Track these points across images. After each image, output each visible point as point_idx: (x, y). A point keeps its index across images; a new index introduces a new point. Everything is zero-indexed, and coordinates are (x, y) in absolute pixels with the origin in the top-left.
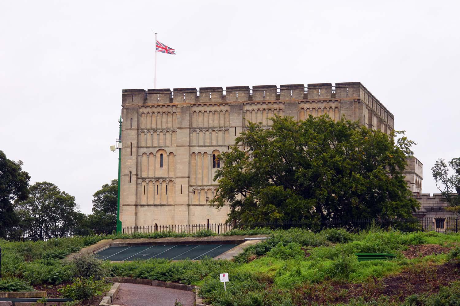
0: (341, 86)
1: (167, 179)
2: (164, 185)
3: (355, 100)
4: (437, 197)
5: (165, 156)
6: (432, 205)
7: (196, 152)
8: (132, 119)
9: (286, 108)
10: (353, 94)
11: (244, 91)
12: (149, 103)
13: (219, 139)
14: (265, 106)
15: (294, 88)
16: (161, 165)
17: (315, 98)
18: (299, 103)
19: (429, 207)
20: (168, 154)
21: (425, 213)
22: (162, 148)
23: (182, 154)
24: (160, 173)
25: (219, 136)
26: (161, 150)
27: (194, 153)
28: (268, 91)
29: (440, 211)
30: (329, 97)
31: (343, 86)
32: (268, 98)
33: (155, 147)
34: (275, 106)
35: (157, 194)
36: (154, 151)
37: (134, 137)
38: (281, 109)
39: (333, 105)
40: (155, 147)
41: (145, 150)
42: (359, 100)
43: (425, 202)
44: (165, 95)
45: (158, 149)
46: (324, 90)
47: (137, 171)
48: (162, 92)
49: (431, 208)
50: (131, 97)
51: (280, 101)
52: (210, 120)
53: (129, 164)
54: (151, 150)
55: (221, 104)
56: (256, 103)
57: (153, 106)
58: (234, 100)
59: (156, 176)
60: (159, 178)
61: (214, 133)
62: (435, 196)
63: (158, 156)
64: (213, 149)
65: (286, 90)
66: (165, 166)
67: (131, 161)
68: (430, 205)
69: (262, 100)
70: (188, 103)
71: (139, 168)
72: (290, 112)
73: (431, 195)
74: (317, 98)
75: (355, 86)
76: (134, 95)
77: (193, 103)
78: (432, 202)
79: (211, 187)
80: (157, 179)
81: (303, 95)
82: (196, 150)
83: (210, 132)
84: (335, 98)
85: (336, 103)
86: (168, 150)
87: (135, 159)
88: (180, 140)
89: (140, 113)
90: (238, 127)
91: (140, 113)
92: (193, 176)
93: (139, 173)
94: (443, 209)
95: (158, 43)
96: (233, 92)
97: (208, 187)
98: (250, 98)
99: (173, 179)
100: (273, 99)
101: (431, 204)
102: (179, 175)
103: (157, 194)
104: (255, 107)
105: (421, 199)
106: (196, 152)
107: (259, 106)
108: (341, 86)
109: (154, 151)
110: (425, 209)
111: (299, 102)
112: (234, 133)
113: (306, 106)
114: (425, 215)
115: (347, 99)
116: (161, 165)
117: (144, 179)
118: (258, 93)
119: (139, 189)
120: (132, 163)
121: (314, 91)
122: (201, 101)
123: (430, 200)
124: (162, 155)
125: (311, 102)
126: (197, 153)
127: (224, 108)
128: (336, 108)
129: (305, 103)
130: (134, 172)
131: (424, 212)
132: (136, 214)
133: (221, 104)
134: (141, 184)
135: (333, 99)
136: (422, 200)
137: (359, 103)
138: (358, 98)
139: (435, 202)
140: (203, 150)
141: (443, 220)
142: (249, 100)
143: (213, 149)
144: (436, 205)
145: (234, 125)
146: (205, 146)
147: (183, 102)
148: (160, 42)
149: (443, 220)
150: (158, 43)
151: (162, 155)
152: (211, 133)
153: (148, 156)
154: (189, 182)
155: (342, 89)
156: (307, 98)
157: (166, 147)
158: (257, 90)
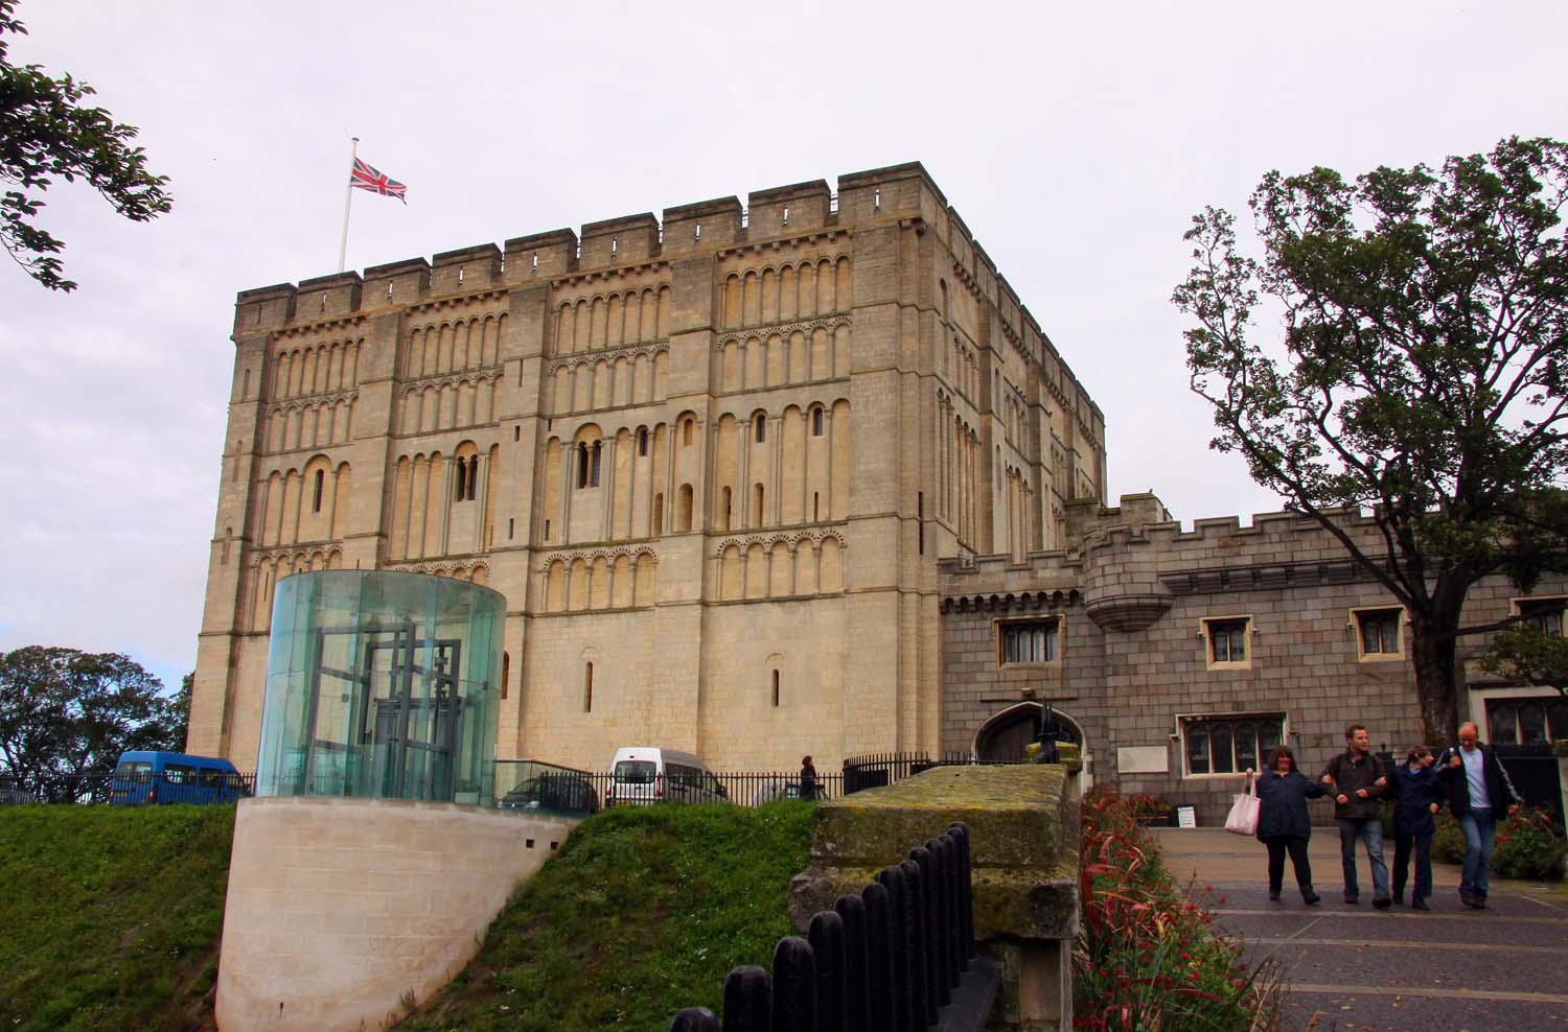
0: (854, 183)
1: (327, 547)
3: (904, 224)
4: (1209, 533)
6: (1192, 566)
7: (411, 453)
8: (248, 371)
9: (676, 276)
10: (898, 203)
11: (558, 243)
12: (300, 322)
13: (479, 404)
14: (616, 285)
15: (706, 211)
16: (317, 508)
17: (771, 234)
18: (722, 260)
19: (1180, 573)
20: (335, 468)
21: (1163, 601)
22: (323, 452)
23: (368, 461)
25: (480, 397)
27: (404, 457)
28: (627, 233)
29: (1226, 587)
30: (817, 226)
31: (864, 182)
32: (625, 255)
33: (305, 450)
34: (649, 279)
37: (249, 424)
38: (664, 287)
39: (831, 250)
40: (305, 450)
42: (917, 221)
43: (1162, 557)
44: (342, 292)
45: (310, 455)
46: (800, 203)
47: (248, 524)
48: (334, 284)
49: (1187, 577)
50: (254, 310)
51: (660, 259)
52: (457, 351)
55: (488, 295)
56: (588, 278)
57: (308, 328)
58: (527, 277)
59: (301, 540)
60: (305, 546)
61: (464, 389)
62: (1203, 527)
63: (312, 476)
64: (456, 438)
65: (681, 223)
66: (326, 507)
67: (233, 496)
68: (1186, 566)
69: (607, 264)
70: (399, 306)
71: (258, 519)
72: (690, 287)
73: (1187, 527)
74: (777, 234)
75: (903, 175)
77: (410, 303)
78: (1191, 555)
81: (732, 232)
82: (410, 447)
83: (455, 385)
84: (836, 224)
85: (842, 242)
86: (336, 456)
87: (243, 492)
89: (276, 355)
90: (529, 357)
91: (276, 355)
92: (398, 533)
93: (256, 534)
94: (1236, 577)
95: (358, 163)
96: (525, 253)
97: (436, 563)
98: (573, 264)
100: (641, 256)
101: (1189, 560)
102: (355, 529)
104: (586, 291)
105: (1147, 543)
106: (411, 453)
107: (601, 287)
108: (854, 183)
109: (298, 462)
110: (1166, 583)
111: (722, 255)
112: (518, 379)
113: (740, 266)
114: (1168, 608)
115: (875, 223)
116: (317, 508)
117: (265, 553)
118: (598, 243)
119: (251, 584)
120: (236, 504)
121: (770, 211)
122: (434, 295)
123: (1183, 545)
124: (320, 473)
125: (757, 248)
126: (411, 458)
127: (496, 307)
128: (842, 258)
129: (741, 256)
130: (238, 532)
131: (1160, 597)
132: (233, 662)
133: (488, 295)
134: (260, 567)
135: (831, 231)
136: (1152, 547)
137: (920, 233)
138: (913, 214)
139: (1202, 554)
140: (429, 444)
141: (1238, 625)
142: (569, 271)
143: (456, 438)
144: (1210, 564)
145: (518, 352)
146: (436, 432)
147: (385, 305)
148: (366, 161)
149: (1238, 625)
150: (358, 163)
151: (320, 473)
152: (456, 390)
153: (285, 480)
154: (380, 549)
155: (860, 193)
156: (746, 239)
157: (330, 446)
158: (592, 237)
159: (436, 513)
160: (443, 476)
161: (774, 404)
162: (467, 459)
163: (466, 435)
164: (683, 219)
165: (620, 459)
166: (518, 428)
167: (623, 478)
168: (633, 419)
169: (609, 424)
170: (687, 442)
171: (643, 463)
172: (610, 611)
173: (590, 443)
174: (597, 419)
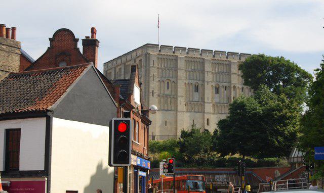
5: (170, 83)
16: (168, 88)
54: (163, 79)
63: (166, 83)
64: (195, 81)
66: (170, 89)
80: (167, 96)
106: (187, 83)
116: (168, 88)
124: (168, 82)
151: (168, 82)
159: (191, 93)
160: (192, 88)
162: (196, 86)
163: (197, 81)
165: (222, 90)
167: (222, 93)
169: (221, 84)
171: (225, 91)
172: (222, 113)
174: (219, 83)
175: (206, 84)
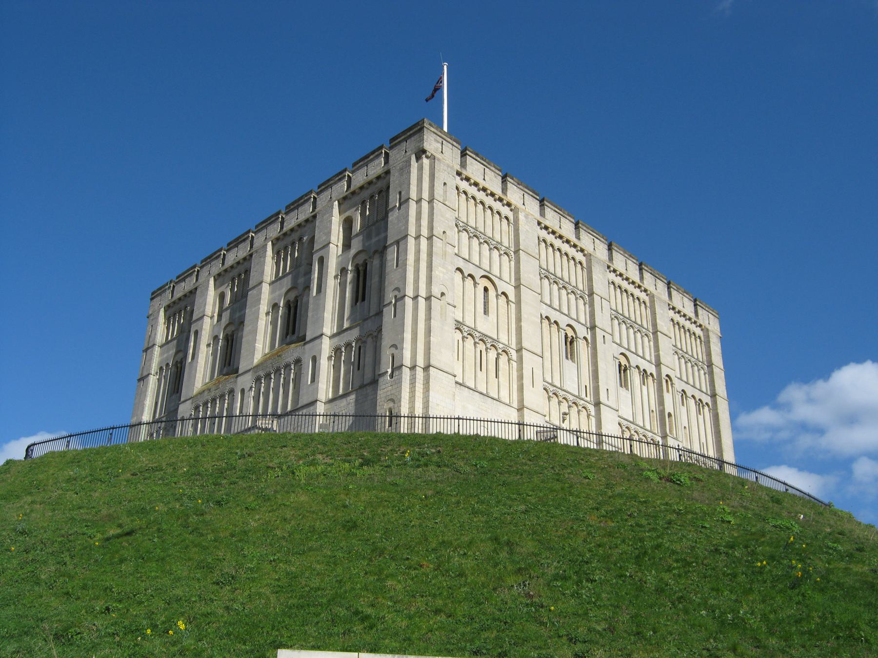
2: (493, 354)
5: (492, 293)
11: (603, 242)
16: (486, 312)
24: (486, 326)
26: (484, 279)
35: (481, 370)
36: (478, 274)
41: (461, 264)
44: (496, 177)
50: (438, 142)
53: (441, 275)
67: (445, 271)
76: (444, 142)
79: (568, 395)
86: (502, 286)
88: (526, 275)
99: (510, 349)
103: (481, 370)
116: (486, 312)
124: (486, 289)
140: (554, 316)
160: (557, 340)
161: (690, 391)
164: (651, 273)
166: (604, 336)
168: (644, 365)
169: (634, 360)
170: (668, 391)
173: (623, 364)
174: (628, 353)
175: (599, 334)
